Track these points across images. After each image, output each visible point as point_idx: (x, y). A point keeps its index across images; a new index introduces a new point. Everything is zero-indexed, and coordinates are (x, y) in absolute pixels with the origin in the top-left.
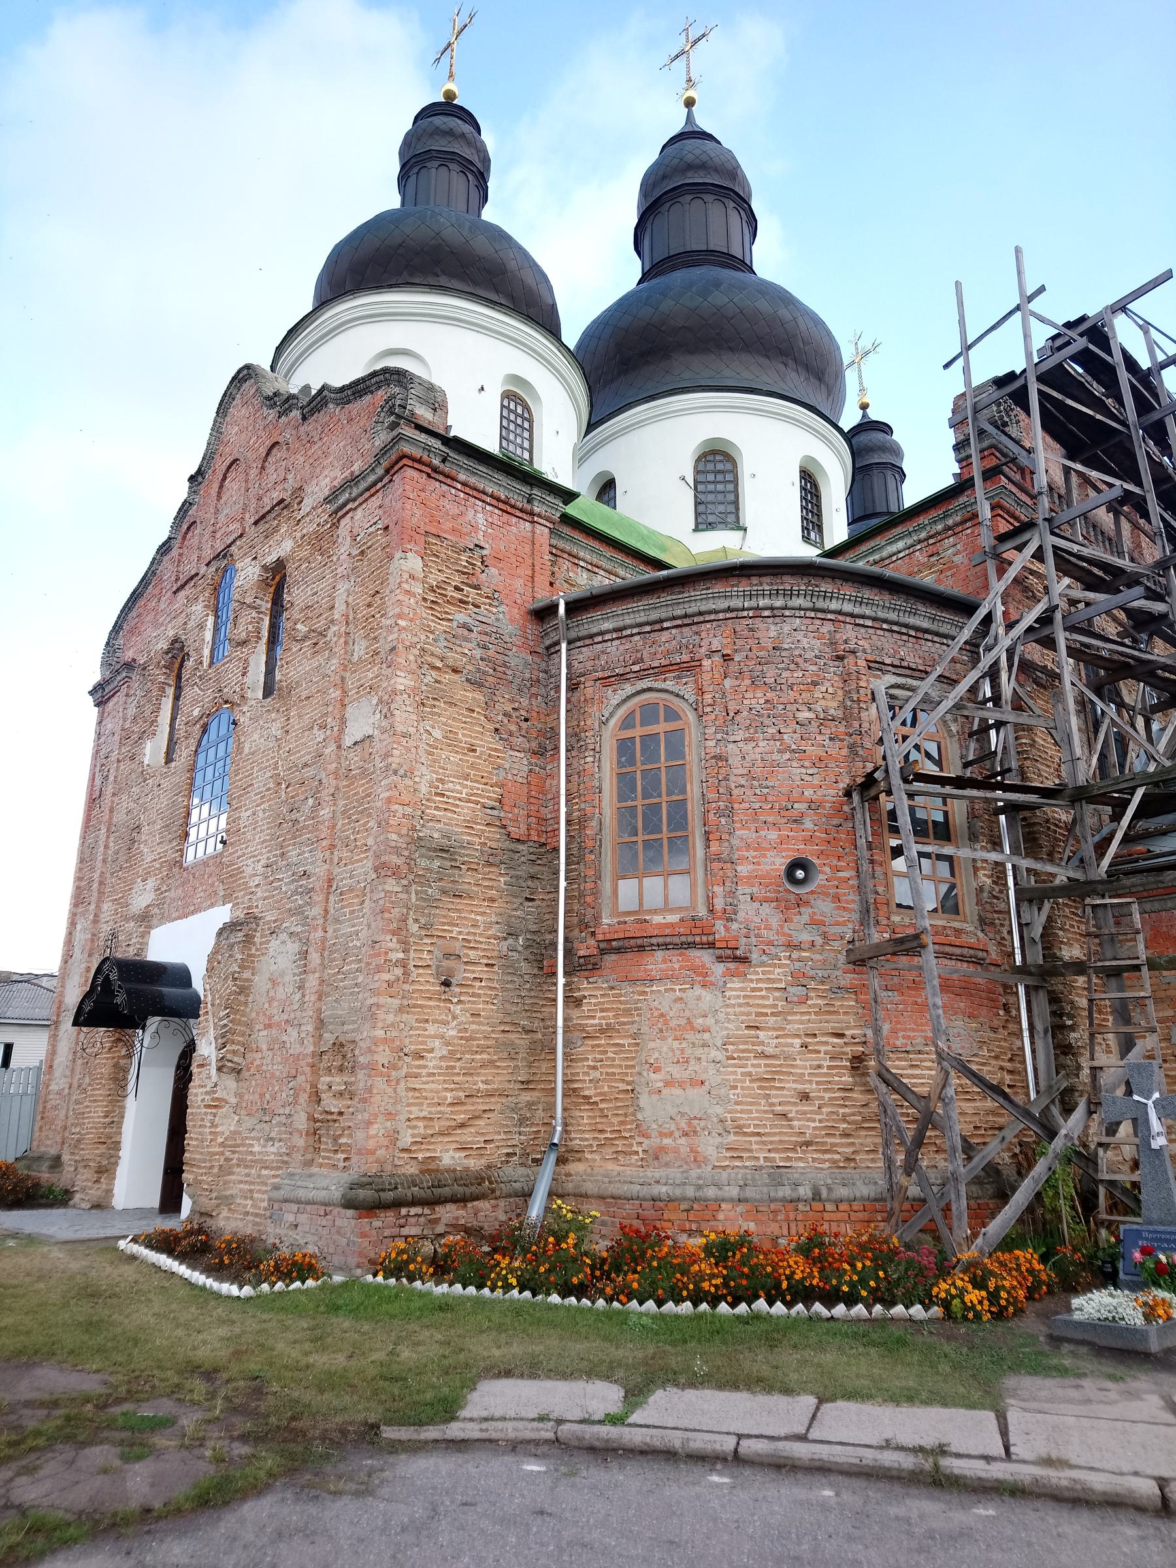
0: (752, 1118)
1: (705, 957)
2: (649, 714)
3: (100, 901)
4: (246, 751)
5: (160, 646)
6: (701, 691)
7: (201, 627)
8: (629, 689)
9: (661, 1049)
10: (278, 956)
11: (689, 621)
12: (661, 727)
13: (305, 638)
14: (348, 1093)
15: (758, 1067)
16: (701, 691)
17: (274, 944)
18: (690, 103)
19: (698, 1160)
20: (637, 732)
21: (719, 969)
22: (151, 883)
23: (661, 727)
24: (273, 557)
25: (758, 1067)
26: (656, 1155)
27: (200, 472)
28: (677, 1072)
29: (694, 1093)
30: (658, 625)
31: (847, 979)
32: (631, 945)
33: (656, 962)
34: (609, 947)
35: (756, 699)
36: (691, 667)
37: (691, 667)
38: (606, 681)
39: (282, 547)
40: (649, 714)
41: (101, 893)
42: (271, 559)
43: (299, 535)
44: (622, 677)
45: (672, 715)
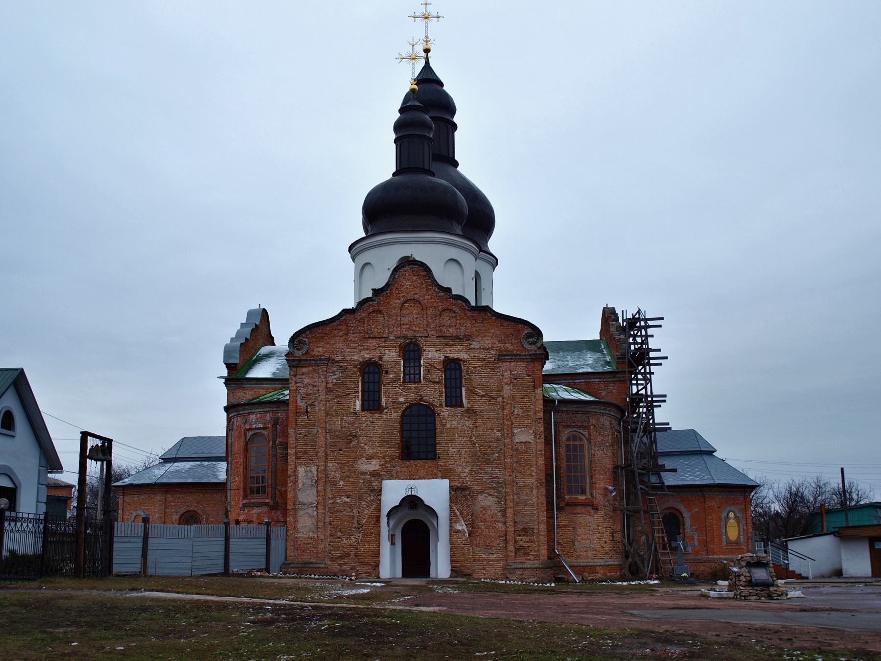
0: (598, 547)
1: (590, 508)
2: (575, 438)
3: (326, 461)
4: (448, 426)
5: (356, 358)
6: (589, 435)
7: (397, 363)
8: (570, 430)
9: (580, 531)
10: (486, 501)
11: (586, 413)
12: (577, 443)
13: (483, 396)
14: (531, 541)
15: (598, 535)
16: (589, 435)
17: (480, 497)
18: (427, 51)
19: (588, 557)
20: (571, 443)
21: (592, 511)
22: (374, 462)
23: (577, 443)
24: (455, 356)
25: (598, 535)
26: (578, 557)
27: (382, 290)
28: (584, 537)
29: (588, 542)
30: (577, 412)
31: (611, 514)
32: (575, 504)
33: (579, 509)
34: (568, 504)
35: (599, 439)
36: (587, 428)
37: (587, 428)
38: (564, 427)
39: (458, 353)
40: (575, 438)
41: (327, 459)
42: (451, 356)
43: (472, 355)
44: (569, 426)
45: (581, 440)
